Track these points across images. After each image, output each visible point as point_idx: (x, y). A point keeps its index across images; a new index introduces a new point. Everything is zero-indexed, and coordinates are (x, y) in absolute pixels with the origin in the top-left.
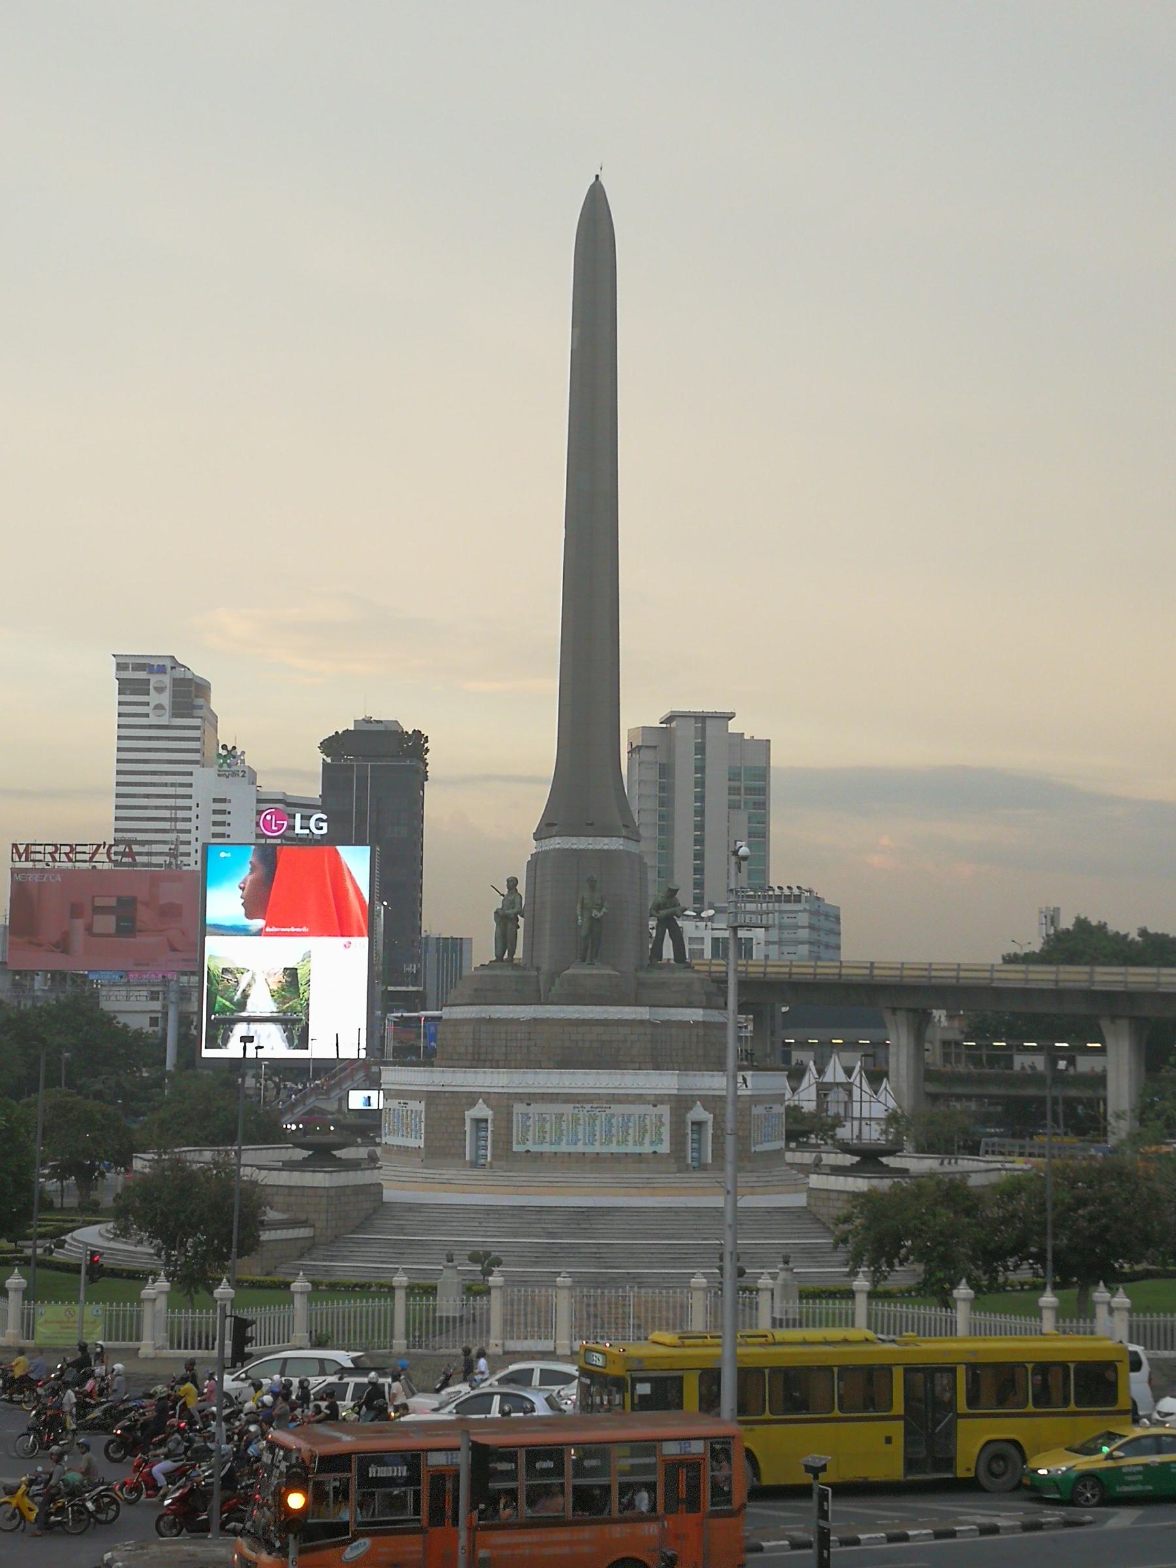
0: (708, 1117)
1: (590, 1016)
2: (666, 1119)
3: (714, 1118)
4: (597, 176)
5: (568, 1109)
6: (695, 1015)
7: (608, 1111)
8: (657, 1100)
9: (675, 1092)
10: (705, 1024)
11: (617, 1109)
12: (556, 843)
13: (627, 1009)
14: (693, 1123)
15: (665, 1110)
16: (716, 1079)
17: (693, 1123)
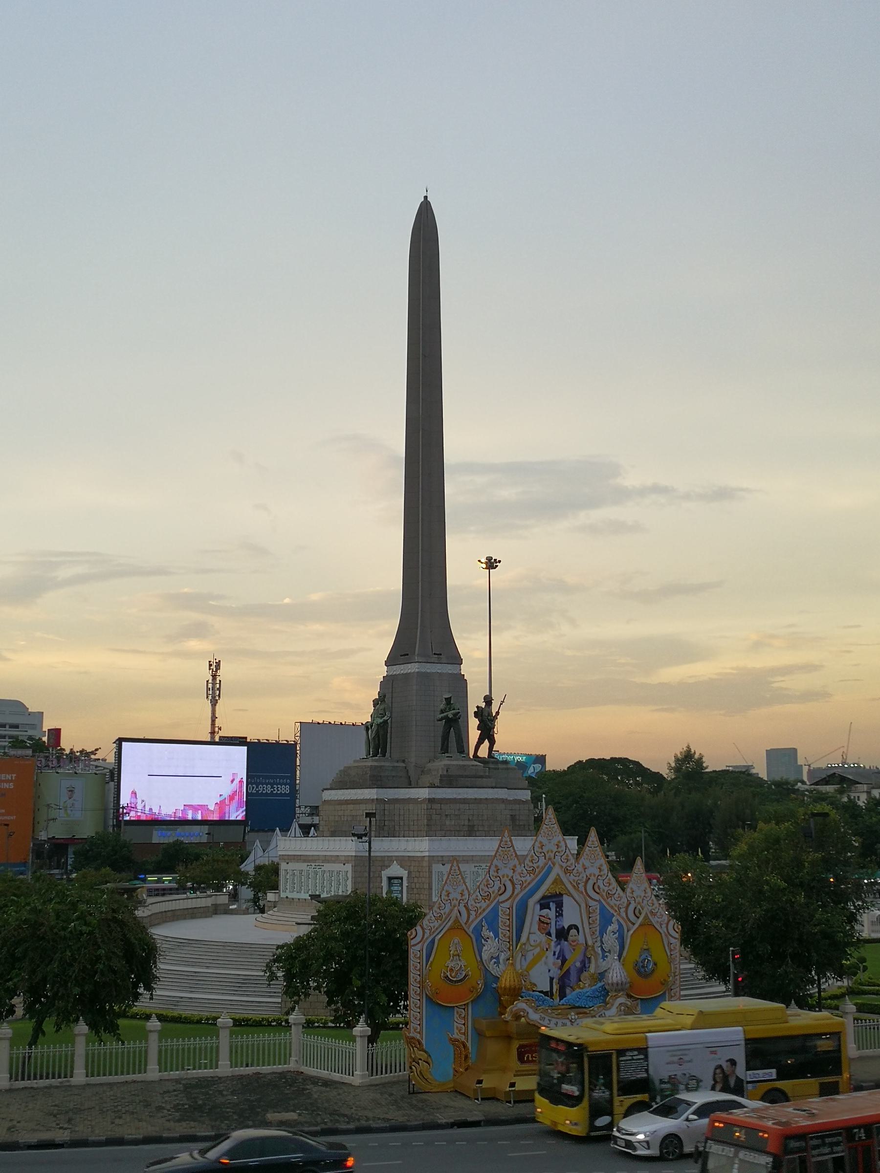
0: (404, 873)
1: (444, 796)
2: (350, 875)
3: (409, 873)
4: (426, 197)
5: (303, 866)
6: (423, 793)
7: (323, 868)
8: (345, 861)
9: (354, 854)
10: (431, 801)
11: (327, 867)
12: (399, 670)
13: (366, 791)
14: (390, 879)
15: (349, 867)
16: (417, 843)
17: (390, 879)
